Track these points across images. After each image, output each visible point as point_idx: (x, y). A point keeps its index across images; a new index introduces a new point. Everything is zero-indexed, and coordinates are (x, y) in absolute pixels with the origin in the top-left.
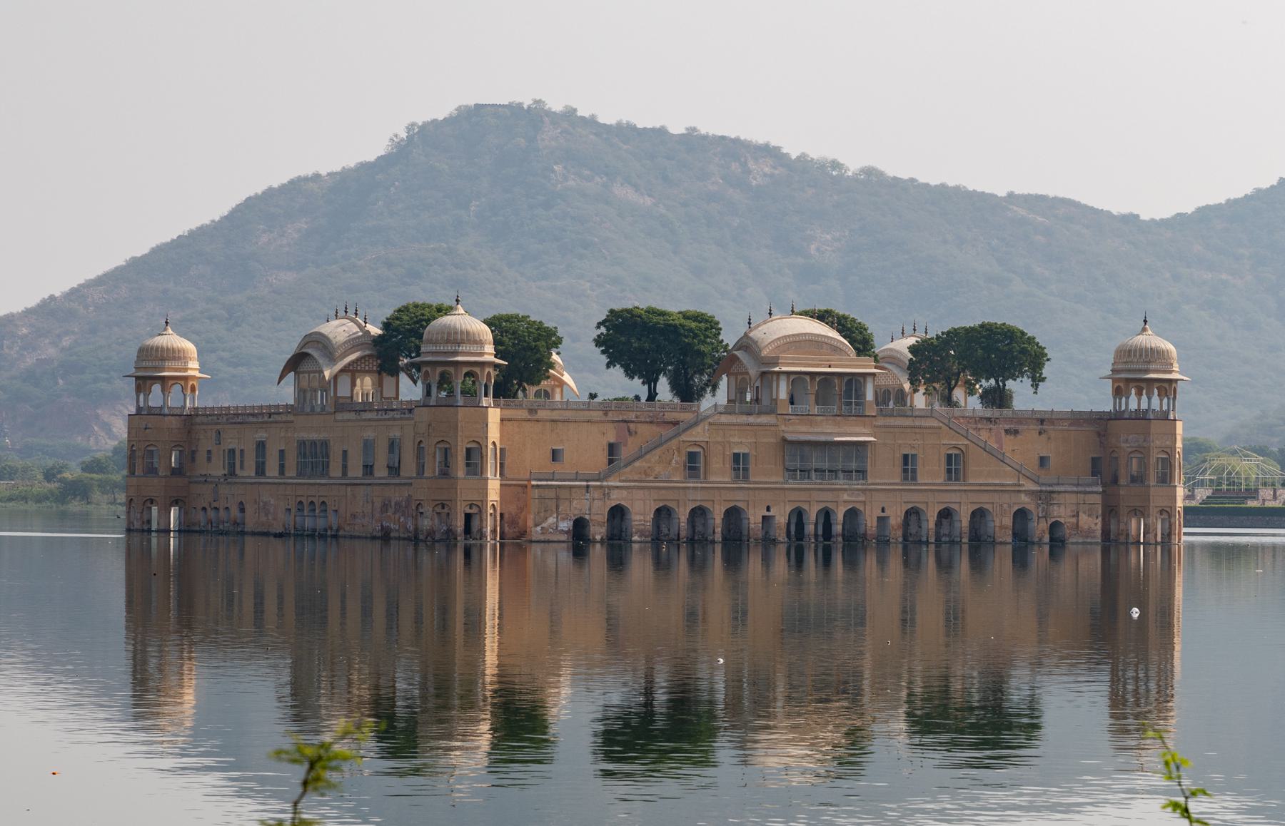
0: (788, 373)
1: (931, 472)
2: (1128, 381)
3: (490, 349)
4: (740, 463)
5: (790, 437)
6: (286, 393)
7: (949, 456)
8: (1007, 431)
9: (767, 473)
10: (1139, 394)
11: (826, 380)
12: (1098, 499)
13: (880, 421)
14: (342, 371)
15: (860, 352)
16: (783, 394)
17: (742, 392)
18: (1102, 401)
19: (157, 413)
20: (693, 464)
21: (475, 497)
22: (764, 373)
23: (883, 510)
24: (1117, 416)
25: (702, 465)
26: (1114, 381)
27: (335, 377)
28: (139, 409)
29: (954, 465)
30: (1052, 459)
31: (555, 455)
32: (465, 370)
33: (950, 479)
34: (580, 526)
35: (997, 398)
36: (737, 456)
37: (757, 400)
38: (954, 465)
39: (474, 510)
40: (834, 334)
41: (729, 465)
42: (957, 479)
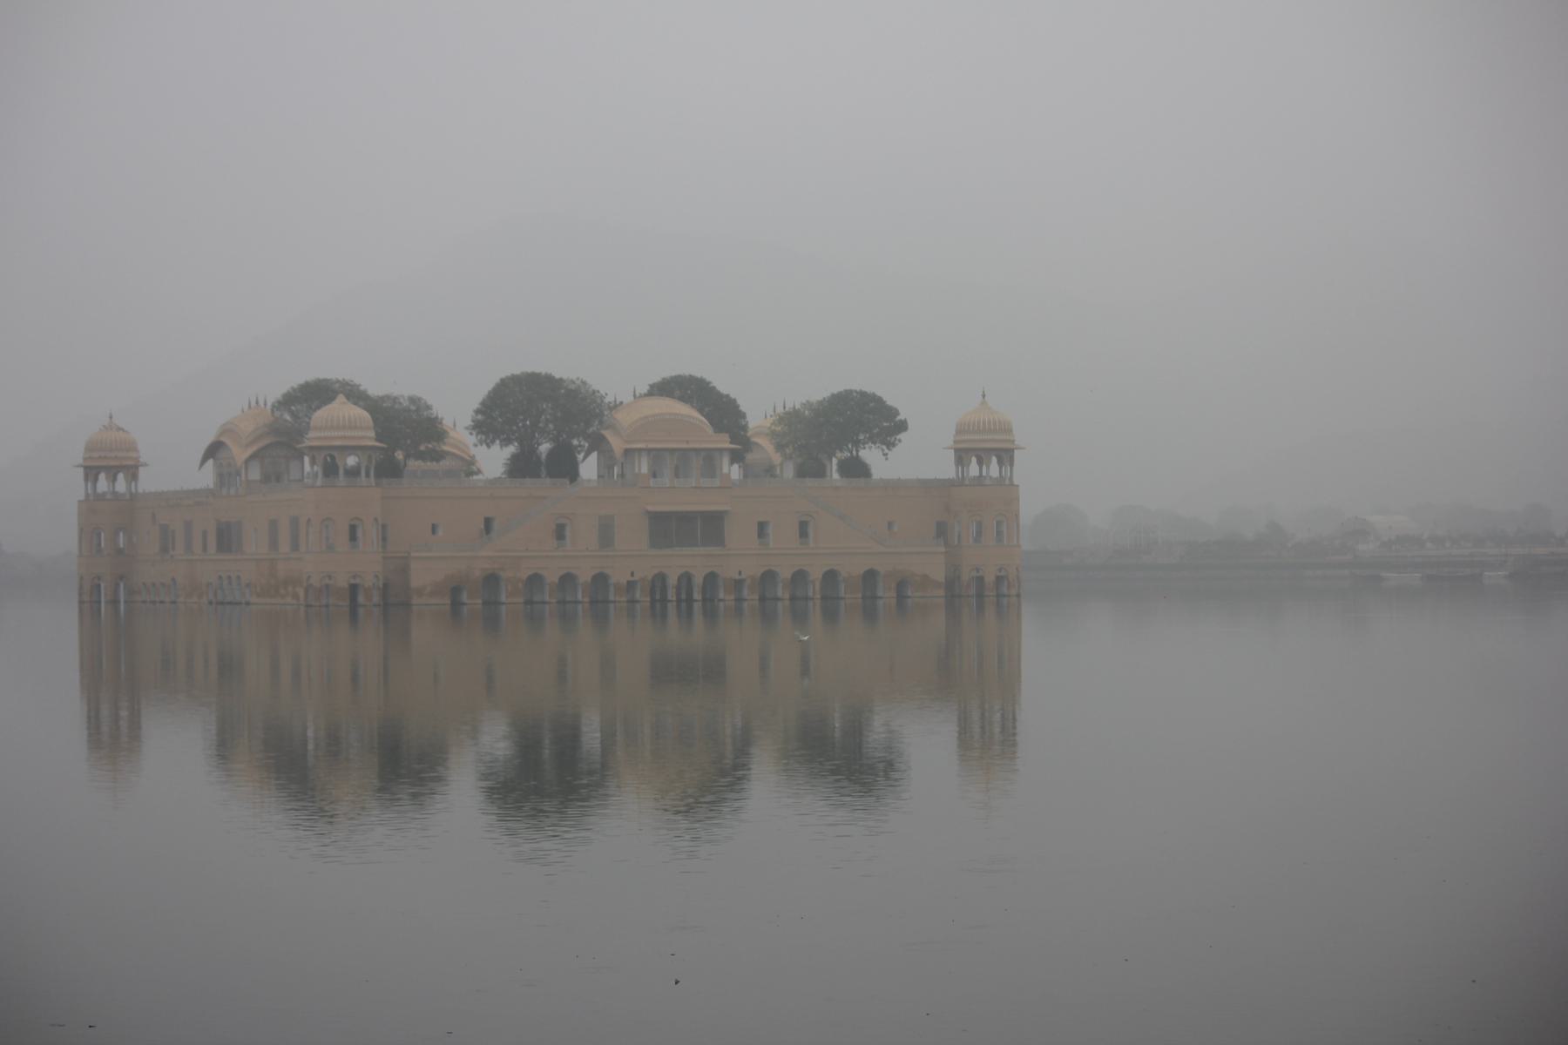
0: (649, 451)
2: (967, 450)
3: (372, 434)
5: (650, 508)
6: (206, 477)
10: (980, 463)
11: (684, 454)
14: (253, 457)
16: (645, 469)
17: (611, 468)
18: (943, 467)
19: (100, 497)
22: (627, 452)
26: (956, 450)
27: (247, 462)
28: (87, 495)
35: (856, 469)
37: (622, 475)
39: (358, 581)
40: (696, 414)
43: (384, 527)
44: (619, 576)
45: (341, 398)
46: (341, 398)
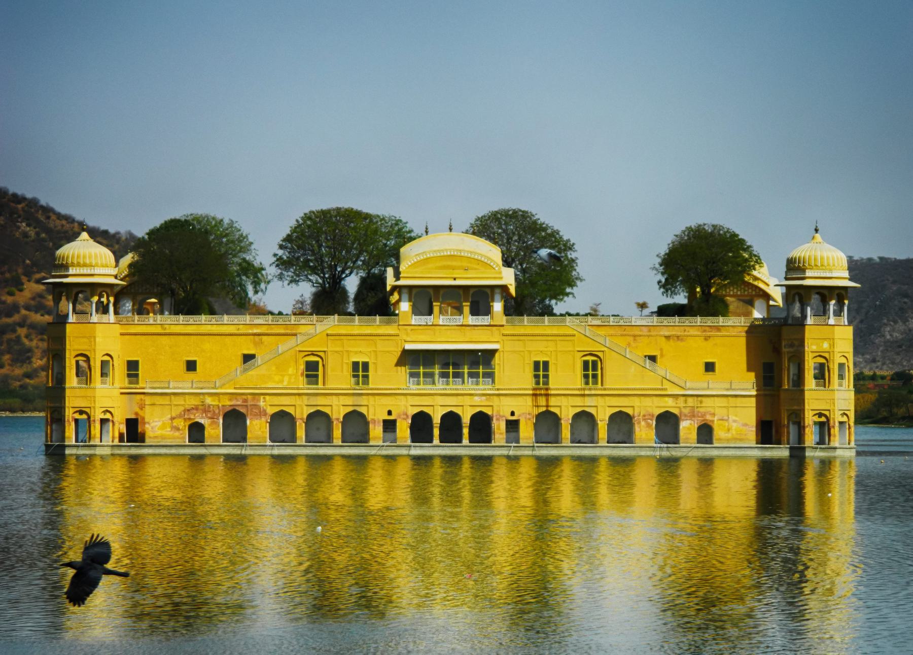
1: (565, 377)
4: (360, 370)
5: (408, 347)
7: (586, 364)
8: (668, 338)
9: (389, 377)
12: (753, 401)
13: (508, 330)
15: (507, 263)
20: (312, 370)
21: (81, 403)
23: (513, 414)
24: (784, 322)
25: (320, 373)
29: (592, 369)
30: (717, 366)
31: (191, 366)
32: (75, 290)
33: (587, 383)
34: (196, 432)
36: (355, 365)
38: (592, 369)
41: (348, 371)
42: (595, 383)
43: (133, 366)
44: (376, 412)
45: (85, 235)
46: (85, 235)
